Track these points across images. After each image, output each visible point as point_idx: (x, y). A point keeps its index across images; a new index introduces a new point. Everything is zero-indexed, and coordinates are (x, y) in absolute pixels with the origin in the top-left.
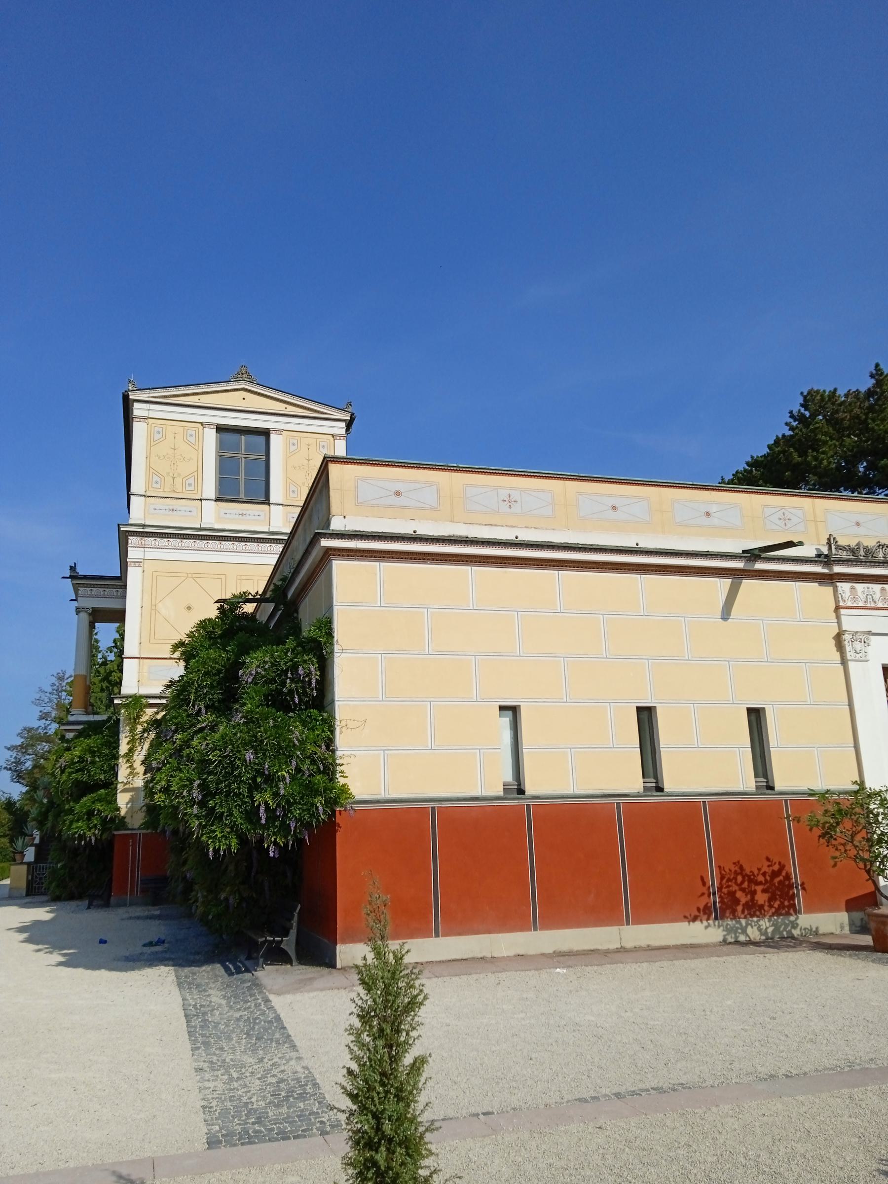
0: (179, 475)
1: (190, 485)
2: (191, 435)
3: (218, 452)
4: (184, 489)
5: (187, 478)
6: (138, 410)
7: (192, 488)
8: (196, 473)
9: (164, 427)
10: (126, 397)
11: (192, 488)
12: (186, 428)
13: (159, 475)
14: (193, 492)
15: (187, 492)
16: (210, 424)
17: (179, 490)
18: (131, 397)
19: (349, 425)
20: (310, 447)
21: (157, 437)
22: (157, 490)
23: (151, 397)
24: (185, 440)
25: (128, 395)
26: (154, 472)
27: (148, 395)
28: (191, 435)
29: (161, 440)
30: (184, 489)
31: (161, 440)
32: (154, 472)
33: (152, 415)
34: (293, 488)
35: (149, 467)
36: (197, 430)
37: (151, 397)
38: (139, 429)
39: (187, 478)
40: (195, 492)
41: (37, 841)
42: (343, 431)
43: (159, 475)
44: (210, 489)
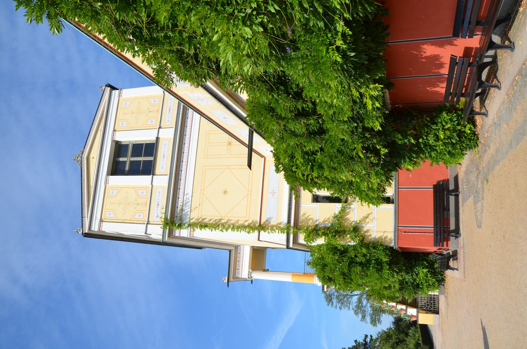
0: (136, 200)
1: (143, 193)
2: (113, 192)
3: (125, 175)
4: (145, 197)
5: (138, 195)
6: (95, 228)
7: (145, 192)
8: (136, 189)
9: (106, 210)
10: (86, 235)
11: (145, 192)
12: (108, 196)
13: (135, 214)
16: (106, 180)
18: (87, 232)
19: (113, 88)
20: (125, 113)
22: (144, 215)
23: (87, 217)
25: (85, 233)
26: (133, 217)
28: (113, 192)
30: (145, 197)
31: (114, 212)
32: (133, 217)
34: (149, 123)
36: (109, 189)
37: (87, 217)
38: (108, 228)
39: (138, 195)
40: (147, 189)
41: (404, 307)
42: (117, 91)
43: (135, 214)
44: (147, 178)
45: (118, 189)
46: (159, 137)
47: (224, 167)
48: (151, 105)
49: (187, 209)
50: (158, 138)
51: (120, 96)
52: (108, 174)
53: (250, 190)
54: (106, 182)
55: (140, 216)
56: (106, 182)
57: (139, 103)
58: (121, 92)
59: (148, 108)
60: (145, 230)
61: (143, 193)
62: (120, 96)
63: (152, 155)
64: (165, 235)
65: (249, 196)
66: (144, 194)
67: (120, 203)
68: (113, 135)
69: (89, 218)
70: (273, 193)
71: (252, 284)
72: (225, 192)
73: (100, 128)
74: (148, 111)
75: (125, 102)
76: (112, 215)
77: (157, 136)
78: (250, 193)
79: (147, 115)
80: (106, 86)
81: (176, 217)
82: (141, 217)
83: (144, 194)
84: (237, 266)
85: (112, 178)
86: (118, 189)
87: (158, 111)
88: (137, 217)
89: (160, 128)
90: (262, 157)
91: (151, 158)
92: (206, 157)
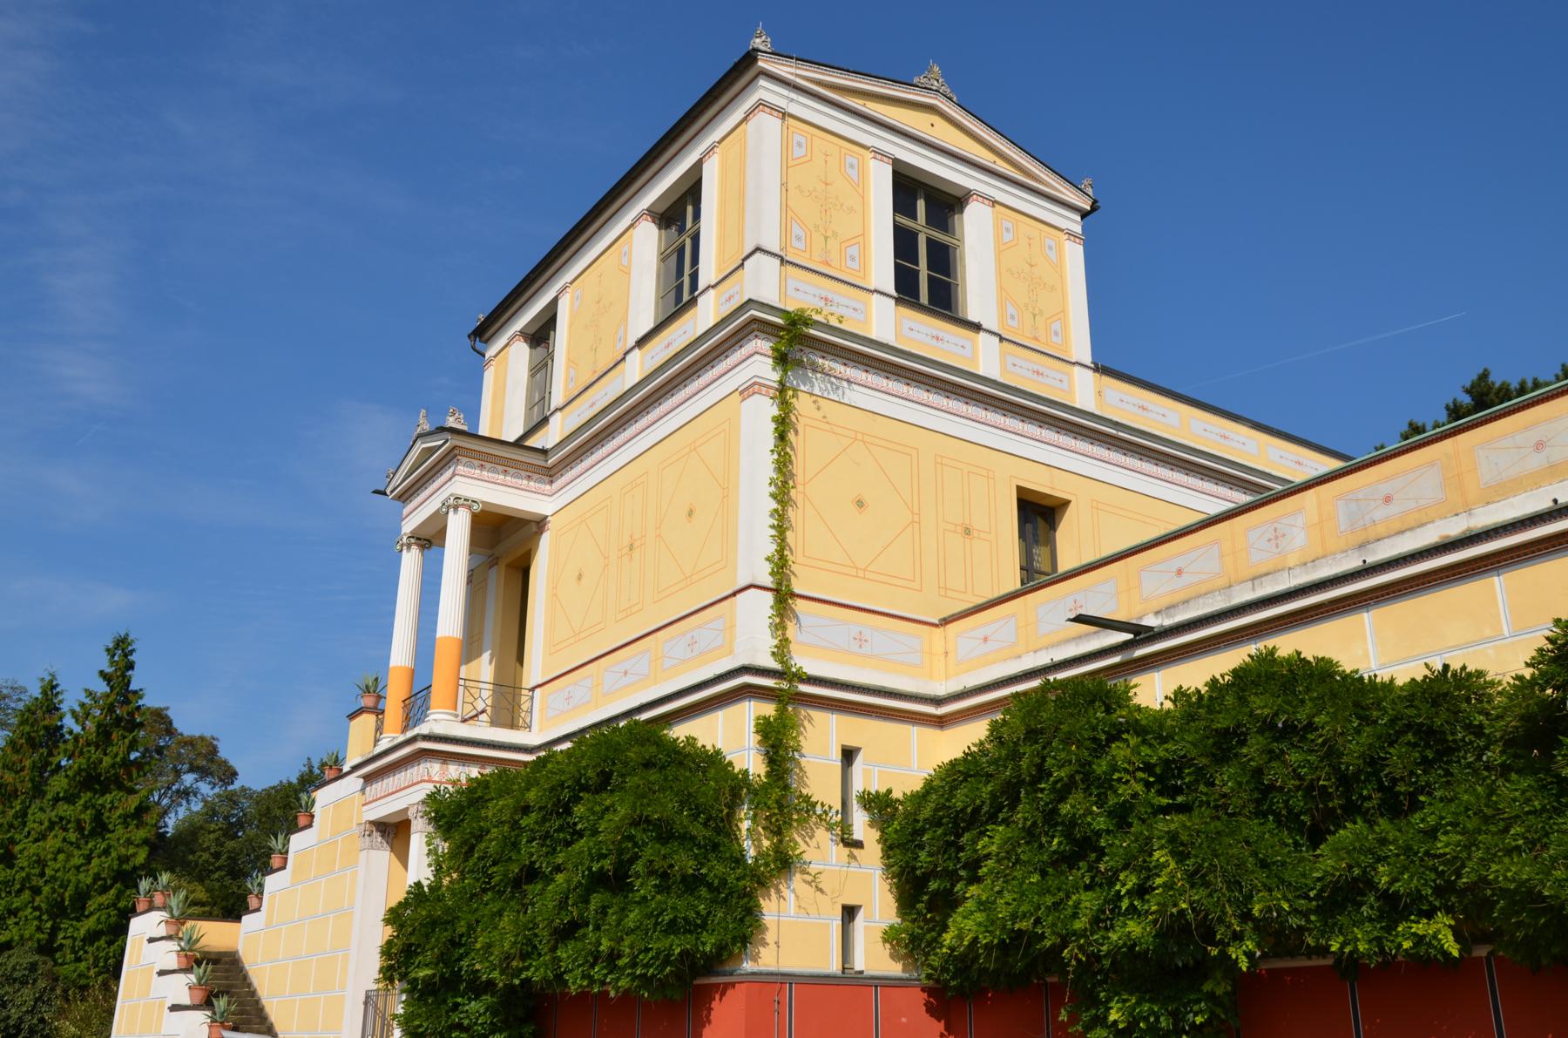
0: (835, 234)
4: (843, 264)
7: (855, 265)
9: (809, 137)
10: (750, 58)
14: (857, 274)
15: (848, 270)
17: (835, 263)
18: (760, 63)
21: (798, 152)
23: (792, 74)
24: (843, 169)
27: (792, 70)
28: (852, 166)
29: (803, 160)
30: (843, 264)
33: (793, 109)
35: (785, 207)
37: (797, 75)
39: (848, 244)
40: (862, 274)
45: (861, 186)
46: (982, 334)
47: (916, 511)
48: (1048, 321)
49: (819, 385)
50: (976, 327)
51: (1070, 234)
52: (897, 163)
53: (869, 575)
54: (878, 153)
55: (799, 238)
56: (878, 153)
57: (1053, 287)
58: (1077, 240)
59: (1041, 312)
60: (767, 249)
61: (853, 259)
62: (1070, 234)
63: (930, 302)
64: (765, 309)
65: (853, 572)
66: (849, 263)
67: (827, 184)
68: (985, 198)
69: (792, 77)
70: (861, 640)
71: (374, 492)
72: (860, 504)
73: (1000, 162)
74: (1037, 311)
75: (847, 166)
76: (798, 152)
77: (984, 326)
78: (861, 574)
79: (1026, 305)
80: (1095, 202)
81: (802, 350)
82: (796, 244)
83: (849, 263)
84: (467, 459)
85: (888, 170)
86: (861, 186)
87: (1036, 339)
88: (797, 230)
89: (1000, 336)
90: (944, 619)
91: (924, 298)
92: (939, 460)
